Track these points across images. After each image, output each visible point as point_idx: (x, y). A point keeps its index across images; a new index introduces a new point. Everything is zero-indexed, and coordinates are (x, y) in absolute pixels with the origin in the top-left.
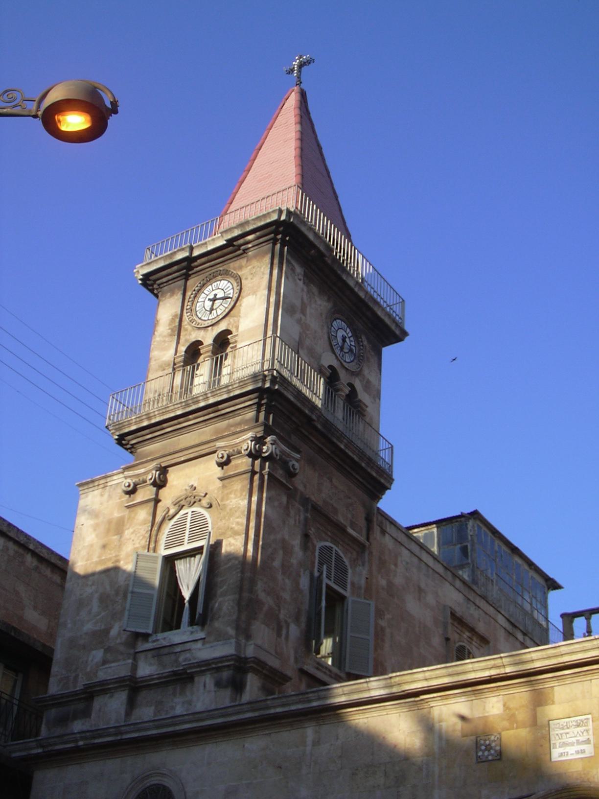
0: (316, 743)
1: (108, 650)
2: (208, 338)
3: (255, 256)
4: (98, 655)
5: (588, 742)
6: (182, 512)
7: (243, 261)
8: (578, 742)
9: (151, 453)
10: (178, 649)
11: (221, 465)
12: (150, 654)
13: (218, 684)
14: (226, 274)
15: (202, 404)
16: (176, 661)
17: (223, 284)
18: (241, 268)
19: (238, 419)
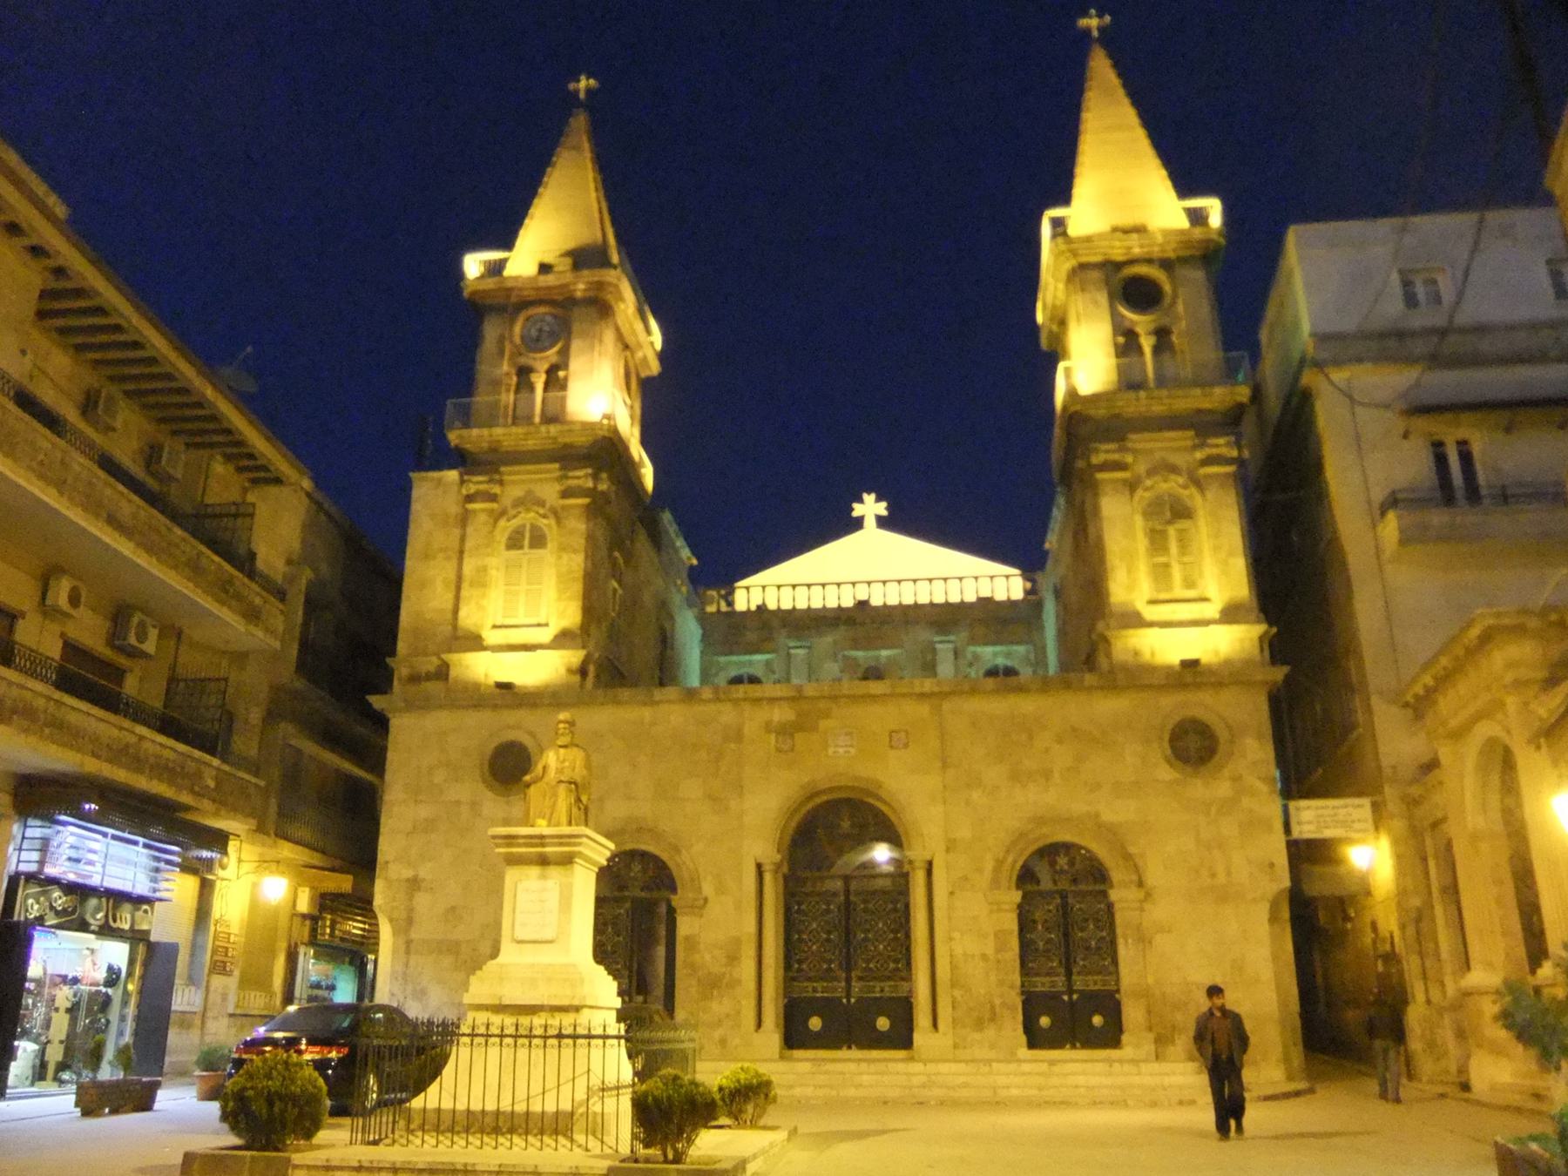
5: (851, 746)
8: (846, 746)
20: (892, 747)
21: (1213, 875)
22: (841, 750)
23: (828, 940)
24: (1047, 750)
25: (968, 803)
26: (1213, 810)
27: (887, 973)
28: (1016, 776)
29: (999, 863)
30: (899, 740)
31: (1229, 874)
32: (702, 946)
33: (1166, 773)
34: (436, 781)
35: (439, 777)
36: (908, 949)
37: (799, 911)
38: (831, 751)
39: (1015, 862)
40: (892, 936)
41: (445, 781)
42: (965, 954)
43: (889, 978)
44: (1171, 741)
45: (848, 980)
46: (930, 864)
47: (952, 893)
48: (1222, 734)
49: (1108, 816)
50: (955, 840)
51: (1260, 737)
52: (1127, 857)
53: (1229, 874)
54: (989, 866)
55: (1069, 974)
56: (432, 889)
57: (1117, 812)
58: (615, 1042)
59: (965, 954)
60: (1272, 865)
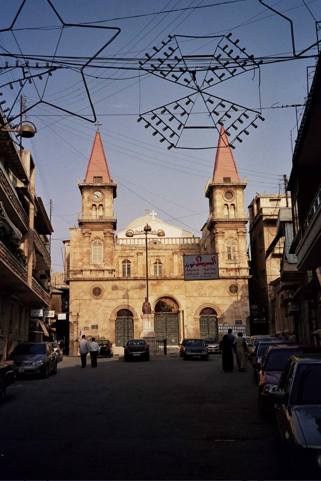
0: (127, 284)
2: (97, 205)
3: (107, 190)
4: (81, 263)
6: (96, 240)
7: (104, 190)
9: (86, 227)
10: (99, 265)
11: (104, 234)
12: (93, 265)
13: (109, 273)
14: (100, 191)
15: (101, 221)
16: (99, 267)
17: (99, 193)
18: (103, 191)
19: (107, 225)
20: (176, 289)
21: (236, 314)
23: (163, 325)
24: (206, 290)
27: (174, 331)
28: (200, 295)
30: (177, 287)
31: (239, 313)
32: (139, 327)
33: (228, 295)
34: (81, 295)
35: (82, 294)
37: (157, 320)
38: (163, 290)
39: (199, 311)
40: (162, 325)
42: (190, 328)
43: (174, 332)
44: (229, 288)
45: (166, 333)
46: (183, 312)
47: (187, 317)
49: (217, 303)
50: (188, 307)
51: (246, 288)
52: (220, 310)
53: (239, 313)
54: (194, 311)
55: (209, 332)
59: (190, 328)
60: (247, 312)
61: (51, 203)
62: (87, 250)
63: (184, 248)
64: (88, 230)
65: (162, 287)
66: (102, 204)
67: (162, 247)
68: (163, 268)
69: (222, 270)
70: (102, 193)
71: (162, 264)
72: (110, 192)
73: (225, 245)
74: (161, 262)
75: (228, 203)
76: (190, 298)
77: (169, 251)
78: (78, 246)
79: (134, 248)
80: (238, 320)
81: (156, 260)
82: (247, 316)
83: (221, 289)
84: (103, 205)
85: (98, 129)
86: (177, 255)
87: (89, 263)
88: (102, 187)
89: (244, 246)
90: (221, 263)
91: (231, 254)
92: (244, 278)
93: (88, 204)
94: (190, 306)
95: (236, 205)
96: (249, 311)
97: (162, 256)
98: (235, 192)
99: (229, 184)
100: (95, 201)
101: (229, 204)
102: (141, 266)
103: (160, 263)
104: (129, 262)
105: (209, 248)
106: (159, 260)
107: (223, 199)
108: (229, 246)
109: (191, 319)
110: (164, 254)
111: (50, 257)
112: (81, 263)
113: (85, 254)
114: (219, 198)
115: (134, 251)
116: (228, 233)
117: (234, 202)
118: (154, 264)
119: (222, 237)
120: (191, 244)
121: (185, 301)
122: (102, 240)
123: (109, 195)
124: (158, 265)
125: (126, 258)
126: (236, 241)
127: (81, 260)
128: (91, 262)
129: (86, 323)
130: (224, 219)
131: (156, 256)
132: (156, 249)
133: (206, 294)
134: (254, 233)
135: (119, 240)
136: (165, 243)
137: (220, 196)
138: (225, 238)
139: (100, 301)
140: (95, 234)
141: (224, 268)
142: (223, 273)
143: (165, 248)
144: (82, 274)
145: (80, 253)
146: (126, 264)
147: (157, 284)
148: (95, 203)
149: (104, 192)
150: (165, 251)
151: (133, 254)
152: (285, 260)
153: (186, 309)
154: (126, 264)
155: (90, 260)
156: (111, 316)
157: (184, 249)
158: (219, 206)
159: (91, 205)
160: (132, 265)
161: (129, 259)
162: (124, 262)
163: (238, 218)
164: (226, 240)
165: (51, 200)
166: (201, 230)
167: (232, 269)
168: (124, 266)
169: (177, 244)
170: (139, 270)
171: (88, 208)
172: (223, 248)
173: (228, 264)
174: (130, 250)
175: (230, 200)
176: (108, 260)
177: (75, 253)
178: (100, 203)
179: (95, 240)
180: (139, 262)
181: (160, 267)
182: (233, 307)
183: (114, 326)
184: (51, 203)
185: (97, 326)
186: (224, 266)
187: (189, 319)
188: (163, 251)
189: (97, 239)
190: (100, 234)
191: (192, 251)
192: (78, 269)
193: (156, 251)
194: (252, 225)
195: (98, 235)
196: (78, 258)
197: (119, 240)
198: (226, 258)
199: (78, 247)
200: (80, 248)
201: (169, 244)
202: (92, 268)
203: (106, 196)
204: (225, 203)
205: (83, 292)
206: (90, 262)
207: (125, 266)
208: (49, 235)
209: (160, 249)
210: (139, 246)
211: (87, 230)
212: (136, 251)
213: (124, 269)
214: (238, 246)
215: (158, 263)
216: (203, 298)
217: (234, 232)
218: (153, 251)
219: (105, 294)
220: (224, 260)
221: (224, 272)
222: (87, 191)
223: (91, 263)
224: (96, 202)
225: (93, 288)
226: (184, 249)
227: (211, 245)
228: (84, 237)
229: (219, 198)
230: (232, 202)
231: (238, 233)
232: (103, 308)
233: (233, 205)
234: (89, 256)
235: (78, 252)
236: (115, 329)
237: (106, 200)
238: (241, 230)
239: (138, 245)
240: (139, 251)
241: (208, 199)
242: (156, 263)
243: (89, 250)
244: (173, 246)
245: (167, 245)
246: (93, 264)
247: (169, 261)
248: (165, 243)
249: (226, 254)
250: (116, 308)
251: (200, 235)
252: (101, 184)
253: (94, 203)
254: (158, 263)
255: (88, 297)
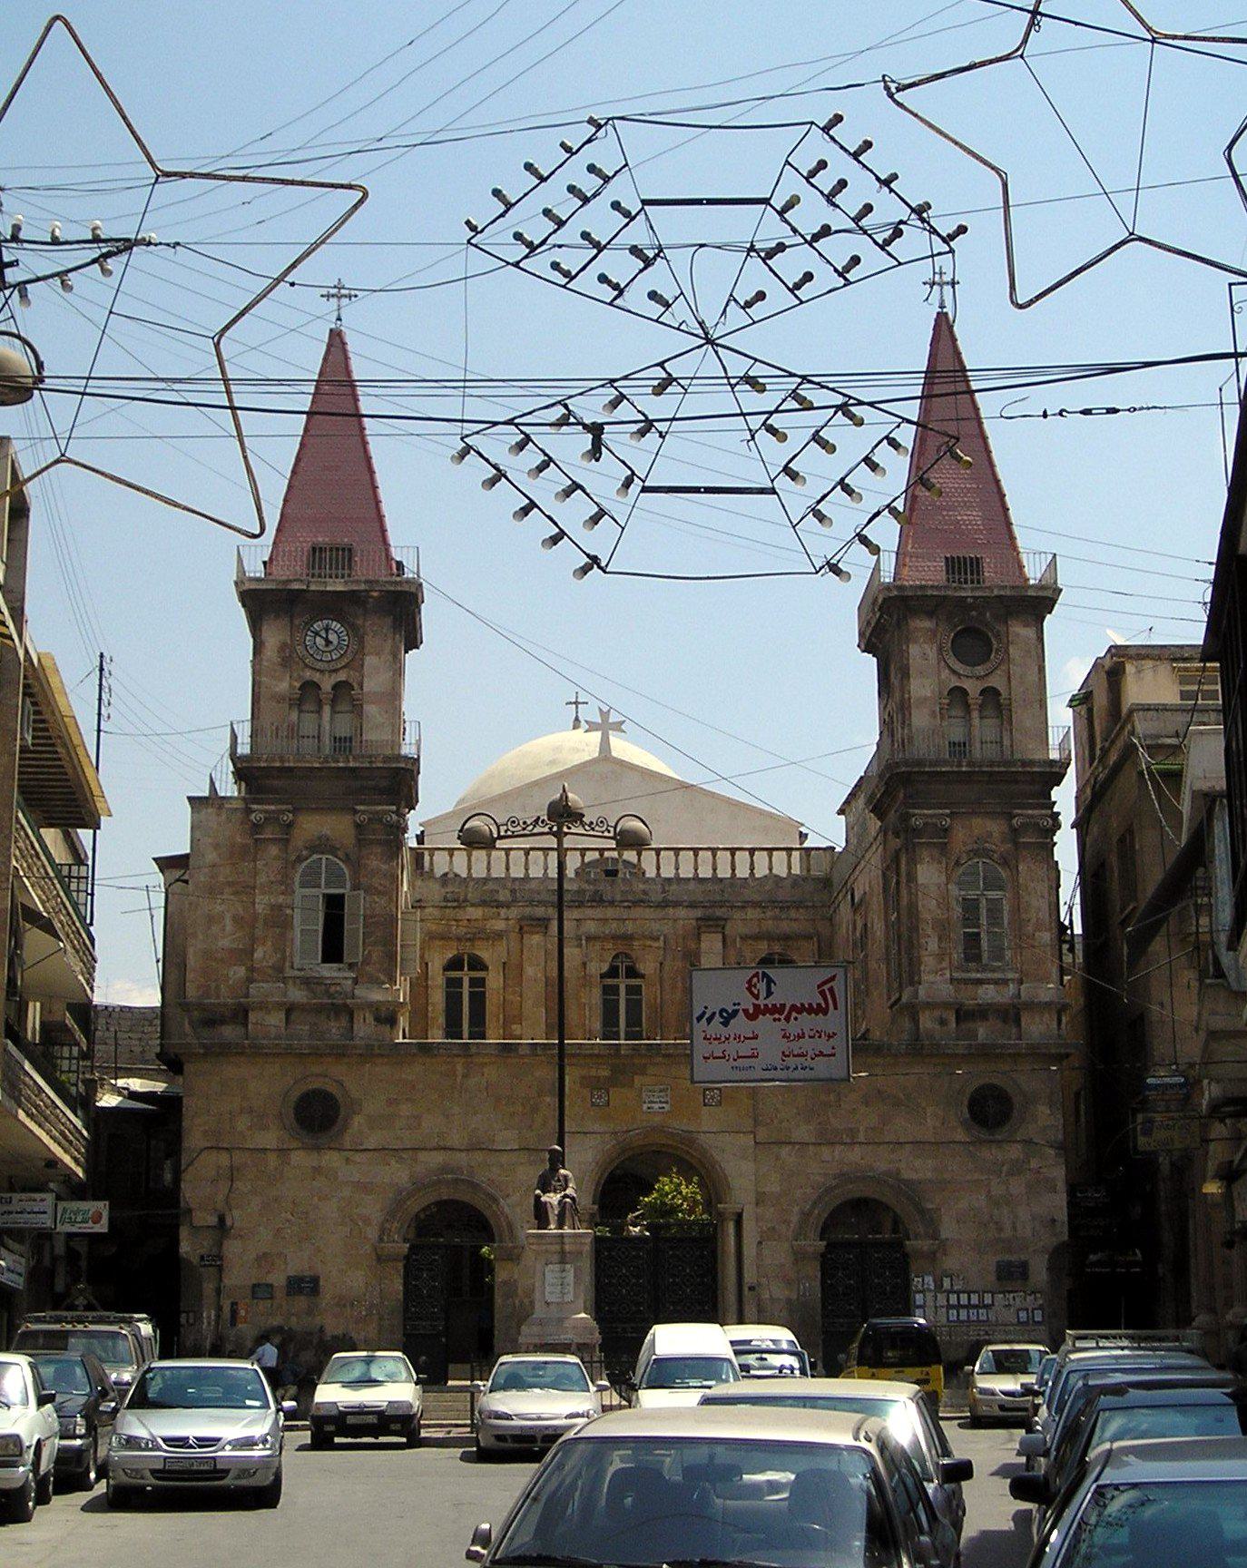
1: (252, 969)
2: (327, 684)
5: (667, 1102)
6: (315, 857)
8: (660, 1102)
11: (358, 826)
12: (298, 981)
16: (327, 991)
17: (335, 625)
21: (1000, 1230)
22: (656, 1106)
25: (778, 1158)
26: (1005, 1168)
29: (805, 1215)
30: (712, 1098)
31: (1014, 1228)
32: (520, 1291)
33: (960, 1135)
35: (242, 1123)
36: (715, 1292)
38: (645, 1106)
41: (250, 1128)
47: (760, 1243)
48: (1017, 1101)
49: (906, 1175)
52: (922, 1212)
53: (1014, 1228)
54: (795, 1219)
56: (241, 1236)
57: (918, 1168)
58: (598, 1365)
60: (1054, 1221)
61: (101, 670)
62: (272, 910)
63: (756, 897)
64: (279, 807)
65: (640, 1096)
66: (351, 681)
67: (645, 892)
68: (647, 995)
69: (937, 1013)
70: (353, 629)
71: (643, 976)
72: (389, 620)
73: (954, 890)
74: (641, 968)
75: (968, 685)
76: (775, 1149)
77: (682, 912)
78: (230, 884)
79: (504, 896)
80: (1007, 1257)
81: (616, 957)
82: (1055, 1241)
83: (929, 1110)
84: (356, 686)
85: (339, 319)
86: (720, 936)
87: (280, 970)
88: (353, 598)
89: (1043, 897)
90: (931, 978)
91: (978, 934)
92: (1040, 1055)
93: (281, 680)
94: (776, 1188)
95: (1004, 694)
96: (1062, 1216)
97: (645, 937)
98: (1002, 628)
99: (973, 589)
100: (320, 665)
101: (973, 688)
102: (540, 987)
103: (632, 972)
104: (477, 964)
105: (876, 903)
106: (627, 956)
107: (943, 663)
108: (972, 894)
109: (778, 1254)
110: (655, 926)
111: (92, 940)
112: (241, 972)
113: (260, 924)
114: (925, 656)
115: (503, 911)
116: (963, 835)
117: (996, 681)
118: (603, 976)
119: (936, 853)
120: (787, 883)
121: (747, 1167)
122: (347, 860)
123: (377, 631)
124: (622, 984)
125: (467, 948)
126: (1004, 874)
127: (244, 954)
128: (292, 967)
129: (259, 1266)
130: (945, 763)
131: (615, 937)
132: (612, 903)
133: (852, 1132)
134: (1095, 830)
135: (431, 856)
136: (658, 874)
137: (932, 652)
138: (954, 858)
139: (331, 1159)
140: (312, 826)
141: (946, 1005)
142: (937, 1027)
143: (660, 898)
144: (245, 1025)
145: (237, 920)
146: (466, 976)
147: (612, 1082)
148: (317, 677)
149: (359, 622)
150: (659, 913)
151: (499, 925)
152: (1217, 977)
153: (757, 1204)
154: (466, 976)
155: (284, 959)
156: (382, 1231)
157: (756, 905)
158: (926, 699)
159: (297, 685)
160: (494, 981)
161: (479, 953)
162: (455, 964)
163: (1017, 756)
164: (957, 864)
165: (102, 656)
166: (841, 812)
167: (981, 1013)
168: (453, 984)
169: (721, 880)
170: (528, 1004)
171: (280, 699)
172: (944, 903)
173: (966, 981)
174: (483, 903)
175: (980, 670)
176: (375, 957)
177: (211, 920)
178: (342, 676)
179: (310, 856)
180: (526, 965)
181: (630, 990)
182: (989, 1196)
183: (398, 1285)
184: (101, 670)
185: (315, 1280)
186: (945, 991)
187: (766, 1252)
188: (649, 913)
189: (323, 853)
190: (336, 826)
191: (793, 914)
192: (226, 997)
193: (610, 912)
194: (1088, 791)
195: (326, 831)
196: (225, 943)
197: (431, 856)
198: (957, 955)
199: (227, 890)
200: (236, 893)
201: (678, 879)
202: (297, 995)
203: (370, 641)
204: (955, 682)
205: (251, 1111)
206: (287, 964)
207: (459, 982)
208: (92, 831)
209: (637, 903)
210: (533, 885)
211: (273, 807)
212: (514, 912)
213: (453, 1001)
214: (1017, 897)
215: (622, 971)
216: (838, 1148)
217: (995, 828)
218: (597, 913)
219: (357, 1121)
220: (944, 964)
221: (943, 1022)
222: (277, 617)
223: (289, 973)
224: (322, 671)
225: (296, 1094)
226: (756, 905)
227: (885, 889)
228: (256, 840)
229: (925, 656)
230: (990, 678)
231: (1014, 831)
232: (346, 1192)
233: (990, 694)
234: (283, 935)
235: (228, 916)
236: (401, 1296)
237: (370, 661)
238: (1032, 816)
239: (526, 879)
240: (528, 911)
241: (869, 665)
242: (613, 972)
243: (280, 907)
244: (702, 887)
245: (669, 880)
246: (297, 973)
247: (679, 964)
248: (658, 874)
249: (959, 932)
250: (410, 1195)
251: (830, 831)
252: (346, 583)
253: (308, 674)
254: (622, 971)
255: (269, 1138)
